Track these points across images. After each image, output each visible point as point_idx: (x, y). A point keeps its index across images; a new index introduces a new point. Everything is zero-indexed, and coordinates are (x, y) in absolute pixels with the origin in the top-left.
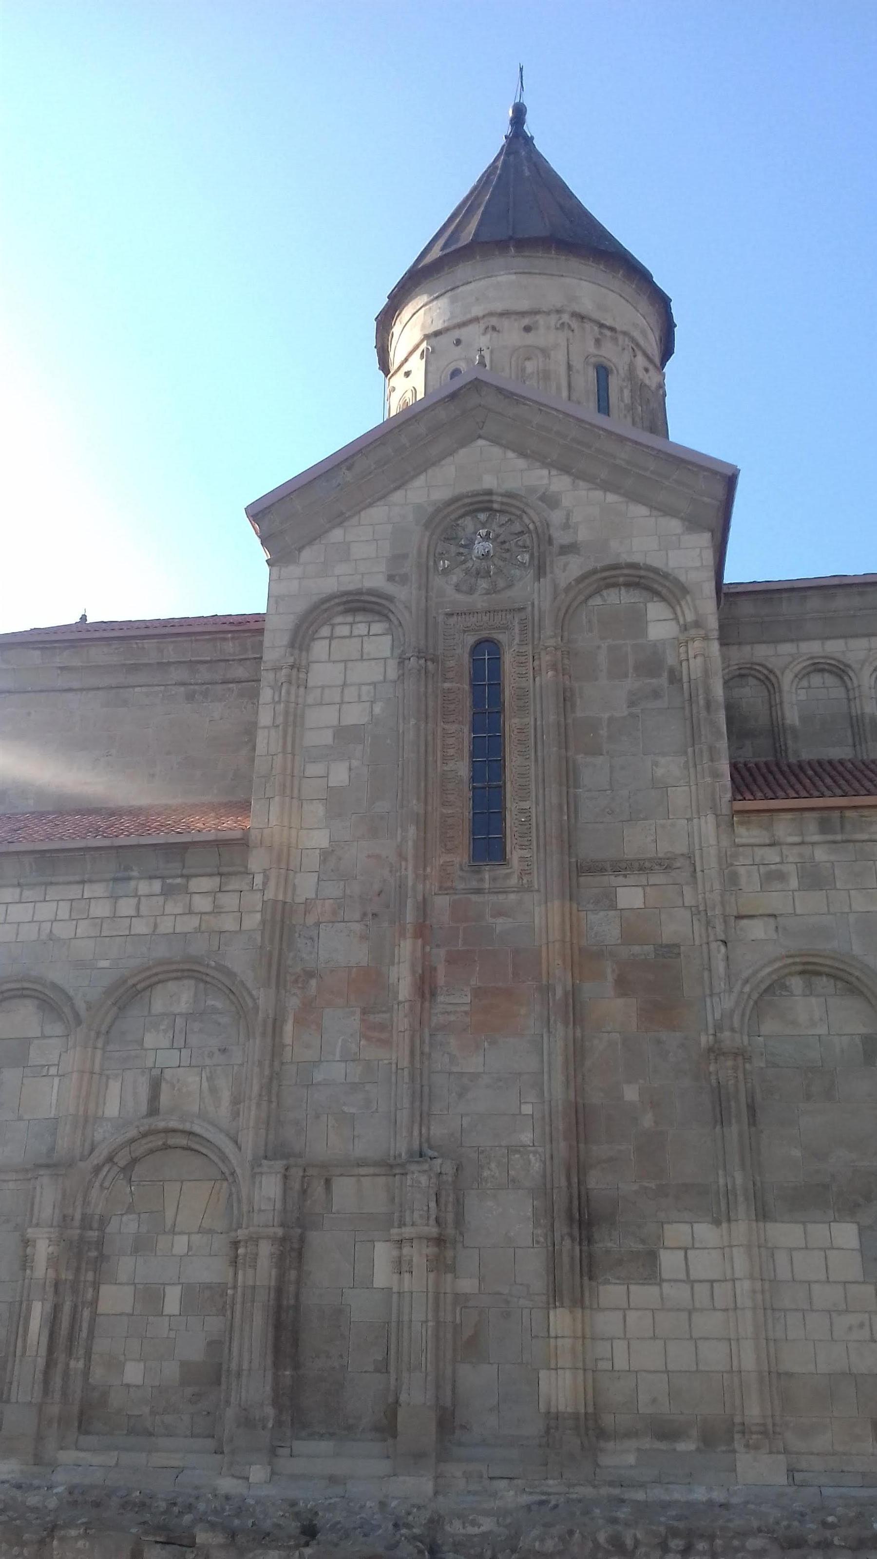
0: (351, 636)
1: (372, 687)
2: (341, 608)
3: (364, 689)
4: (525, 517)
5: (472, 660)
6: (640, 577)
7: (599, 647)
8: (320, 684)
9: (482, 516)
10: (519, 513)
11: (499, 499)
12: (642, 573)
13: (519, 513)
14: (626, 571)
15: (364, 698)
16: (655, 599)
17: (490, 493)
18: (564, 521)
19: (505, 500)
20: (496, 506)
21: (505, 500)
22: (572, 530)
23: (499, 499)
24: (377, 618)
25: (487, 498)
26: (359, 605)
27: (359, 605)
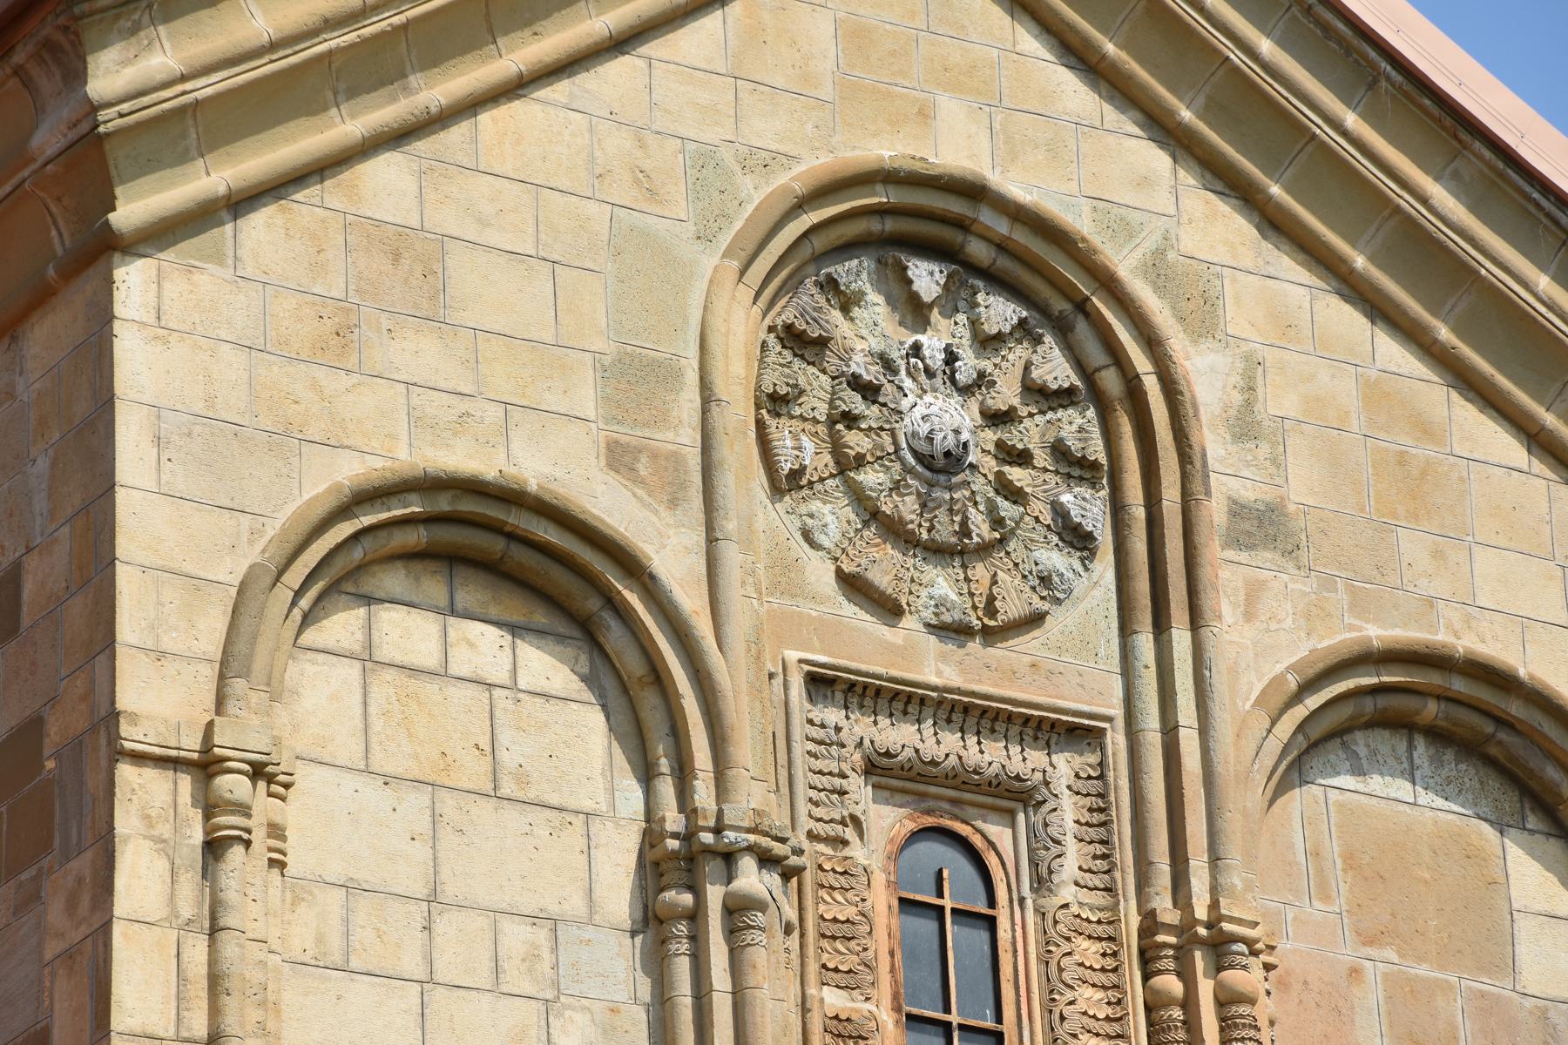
0: (442, 673)
1: (542, 935)
2: (415, 537)
3: (516, 936)
4: (1082, 328)
5: (895, 903)
6: (1502, 722)
7: (1355, 972)
8: (335, 871)
9: (926, 277)
10: (1059, 305)
11: (1002, 227)
12: (1515, 709)
13: (1059, 305)
14: (1459, 685)
15: (516, 980)
16: (1532, 822)
17: (974, 191)
18: (1237, 398)
19: (1022, 237)
20: (978, 250)
21: (1022, 237)
22: (1264, 449)
23: (1002, 227)
24: (541, 617)
25: (955, 206)
26: (496, 545)
27: (496, 545)
